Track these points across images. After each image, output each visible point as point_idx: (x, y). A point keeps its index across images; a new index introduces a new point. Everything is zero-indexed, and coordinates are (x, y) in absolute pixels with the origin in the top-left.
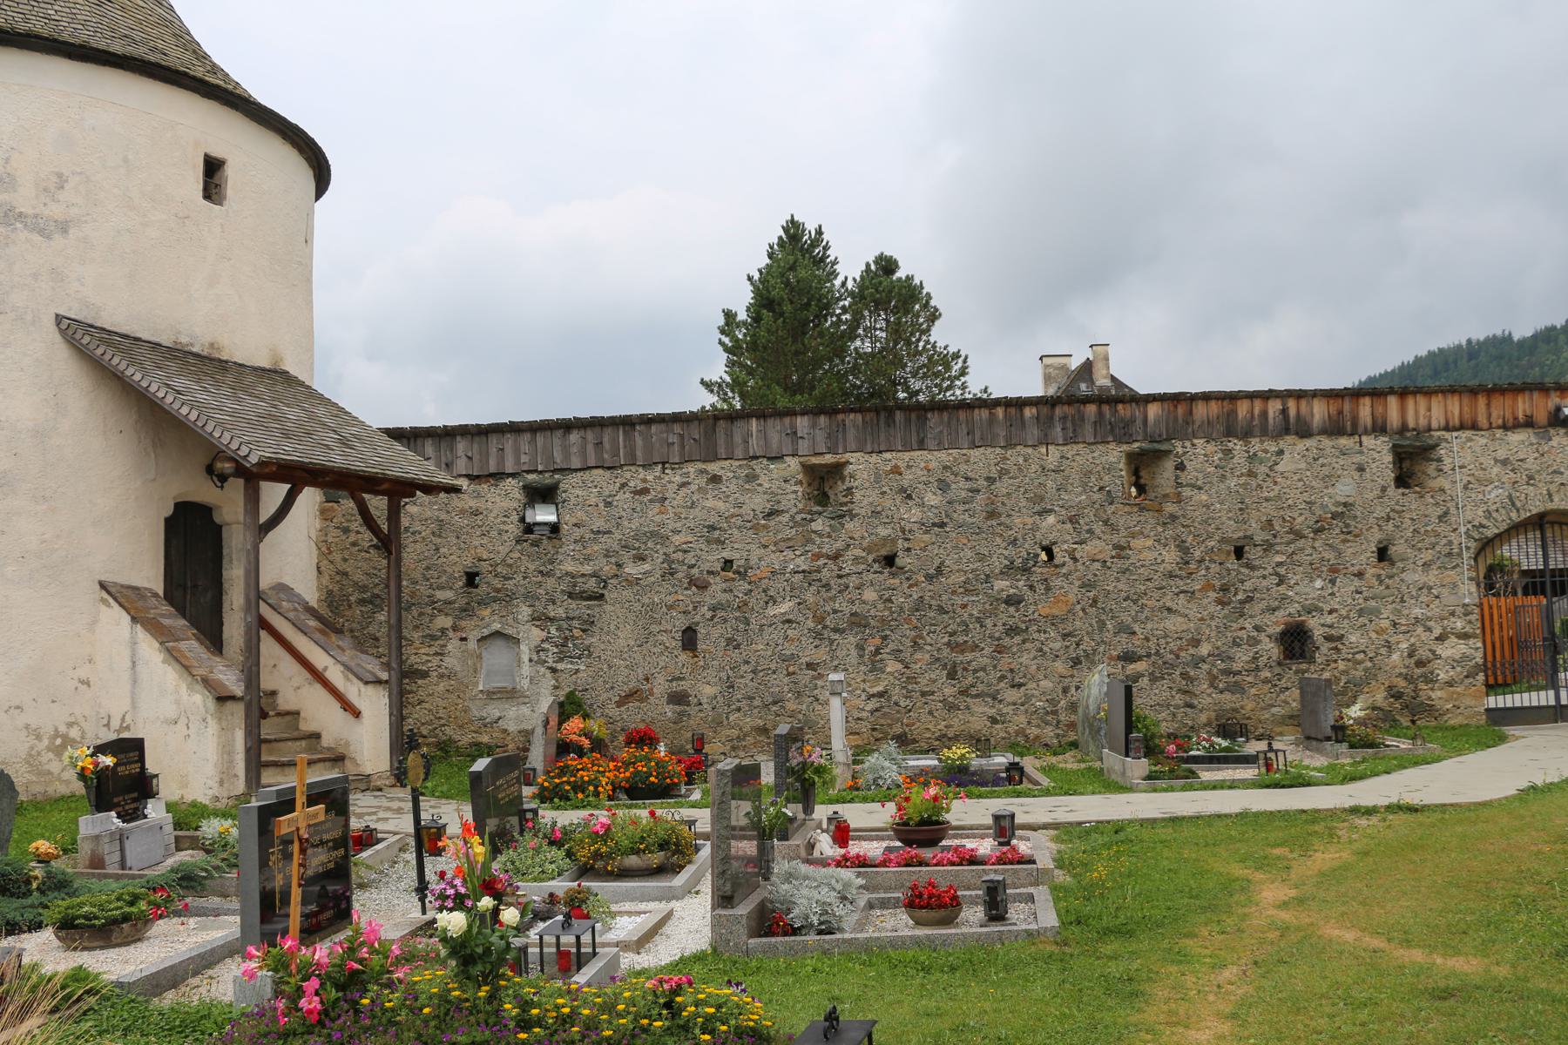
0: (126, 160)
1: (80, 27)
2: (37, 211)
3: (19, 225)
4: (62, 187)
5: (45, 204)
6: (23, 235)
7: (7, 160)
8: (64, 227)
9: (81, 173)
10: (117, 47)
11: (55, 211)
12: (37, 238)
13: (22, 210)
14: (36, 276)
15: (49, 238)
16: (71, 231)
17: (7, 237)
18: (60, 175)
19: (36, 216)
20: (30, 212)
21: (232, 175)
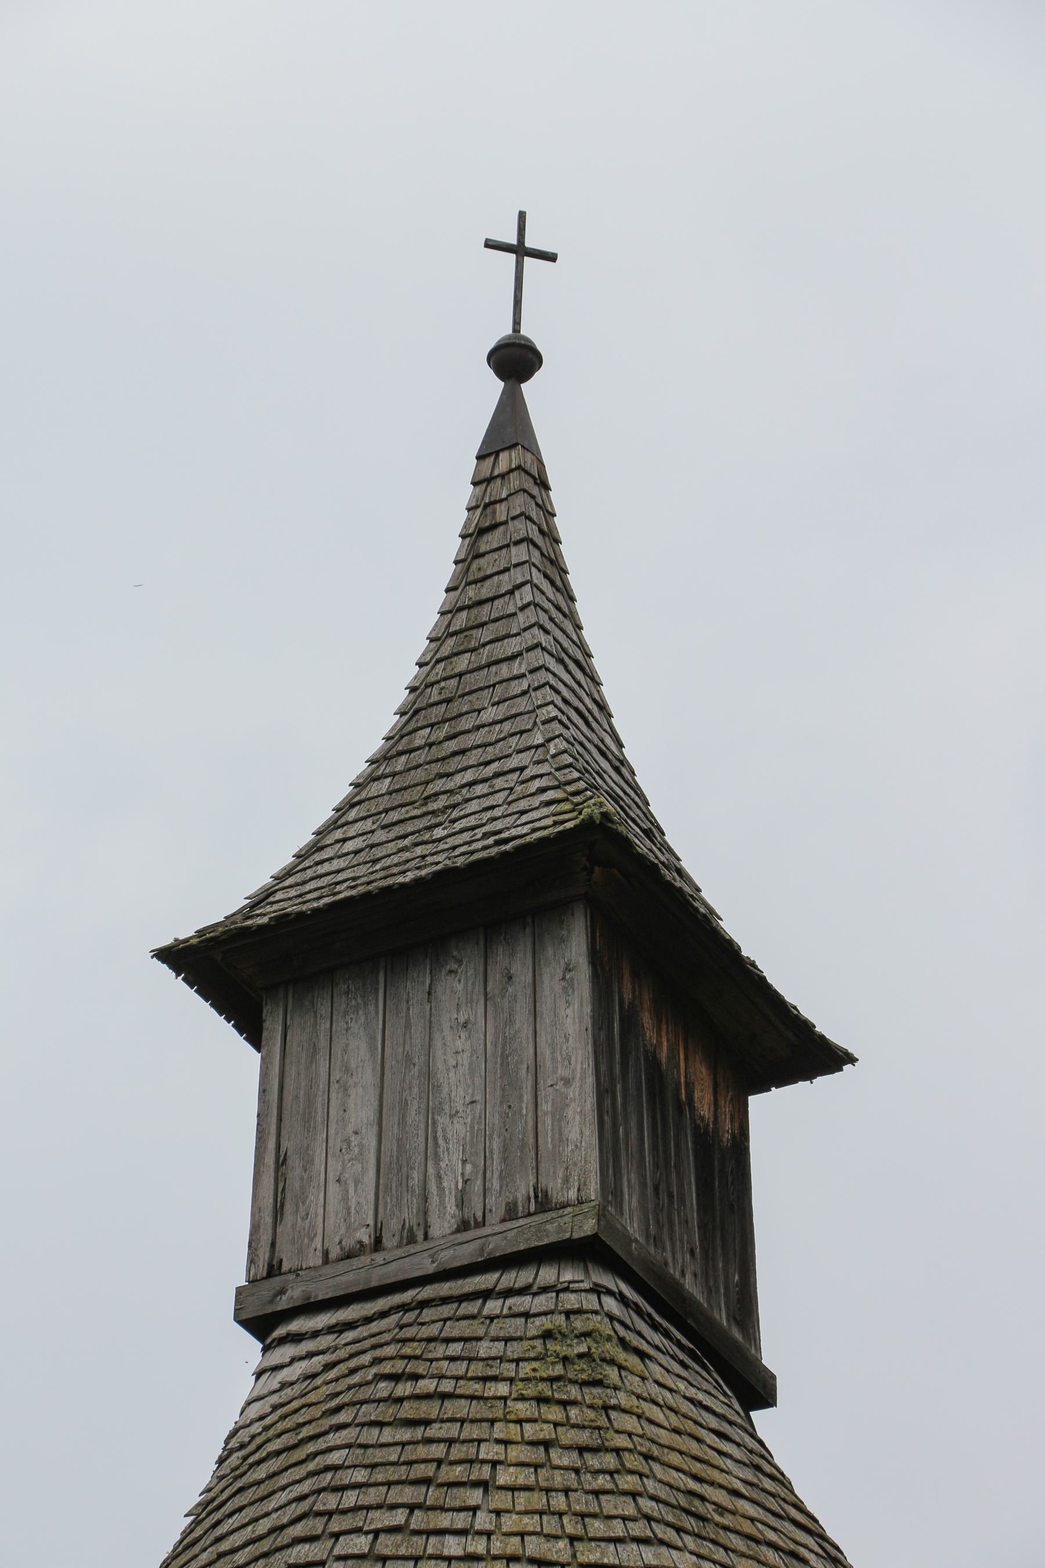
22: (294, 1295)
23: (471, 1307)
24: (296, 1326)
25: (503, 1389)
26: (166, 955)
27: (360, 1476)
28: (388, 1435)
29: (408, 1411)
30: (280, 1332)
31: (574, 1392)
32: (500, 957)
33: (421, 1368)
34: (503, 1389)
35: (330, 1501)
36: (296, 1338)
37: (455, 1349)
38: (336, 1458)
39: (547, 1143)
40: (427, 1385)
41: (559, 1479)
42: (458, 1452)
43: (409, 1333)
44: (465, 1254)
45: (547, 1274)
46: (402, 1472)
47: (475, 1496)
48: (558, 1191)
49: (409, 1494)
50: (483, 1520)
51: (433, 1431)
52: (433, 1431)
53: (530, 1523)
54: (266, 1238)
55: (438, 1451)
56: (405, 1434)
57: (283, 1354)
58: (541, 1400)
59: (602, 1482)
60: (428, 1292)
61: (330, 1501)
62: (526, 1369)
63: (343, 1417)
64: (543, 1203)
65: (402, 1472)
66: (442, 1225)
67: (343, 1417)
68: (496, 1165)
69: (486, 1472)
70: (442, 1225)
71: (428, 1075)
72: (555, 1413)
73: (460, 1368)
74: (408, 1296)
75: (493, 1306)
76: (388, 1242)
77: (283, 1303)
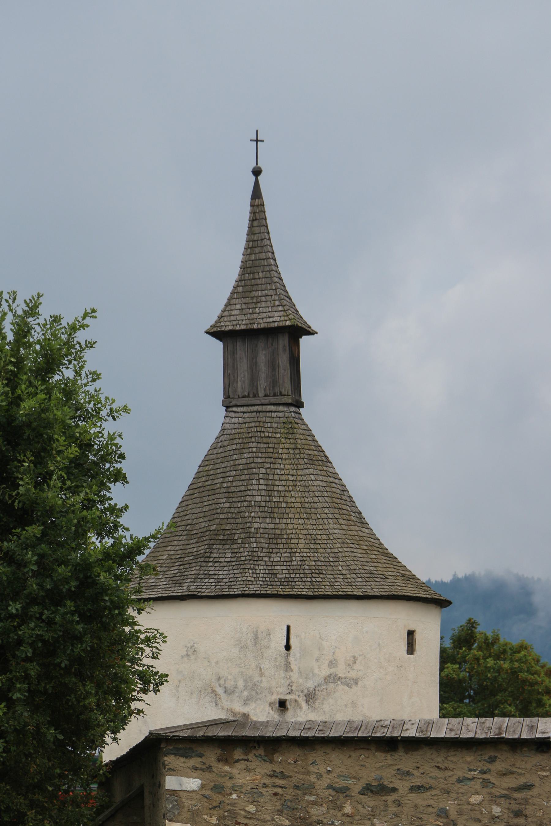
0: (379, 645)
1: (355, 576)
2: (346, 675)
3: (339, 683)
4: (355, 663)
5: (349, 672)
6: (341, 687)
7: (334, 653)
8: (356, 682)
9: (362, 655)
10: (376, 591)
11: (353, 674)
12: (346, 688)
13: (340, 675)
14: (346, 706)
15: (350, 687)
16: (359, 683)
17: (335, 689)
18: (354, 657)
19: (346, 678)
20: (343, 676)
21: (418, 636)
22: (234, 403)
23: (269, 414)
24: (234, 409)
25: (279, 435)
26: (207, 332)
27: (260, 455)
28: (263, 446)
29: (265, 440)
30: (230, 409)
31: (290, 436)
32: (270, 340)
33: (264, 429)
34: (279, 435)
35: (256, 460)
36: (235, 412)
37: (269, 425)
38: (255, 450)
39: (281, 382)
40: (266, 434)
41: (292, 456)
42: (275, 451)
43: (259, 419)
44: (266, 401)
45: (282, 408)
46: (266, 455)
47: (280, 461)
48: (283, 393)
49: (269, 460)
50: (282, 466)
51: (270, 445)
52: (270, 445)
53: (289, 466)
54: (227, 390)
55: (271, 450)
56: (265, 446)
57: (233, 415)
58: (286, 438)
59: (298, 456)
60: (260, 408)
61: (256, 460)
62: (282, 430)
63: (253, 440)
64: (281, 395)
65: (266, 455)
66: (261, 394)
67: (253, 440)
68: (271, 385)
69: (280, 456)
70: (261, 394)
71: (256, 363)
72: (288, 441)
73: (270, 430)
74: (256, 408)
75: (273, 414)
76: (251, 396)
77: (231, 404)
